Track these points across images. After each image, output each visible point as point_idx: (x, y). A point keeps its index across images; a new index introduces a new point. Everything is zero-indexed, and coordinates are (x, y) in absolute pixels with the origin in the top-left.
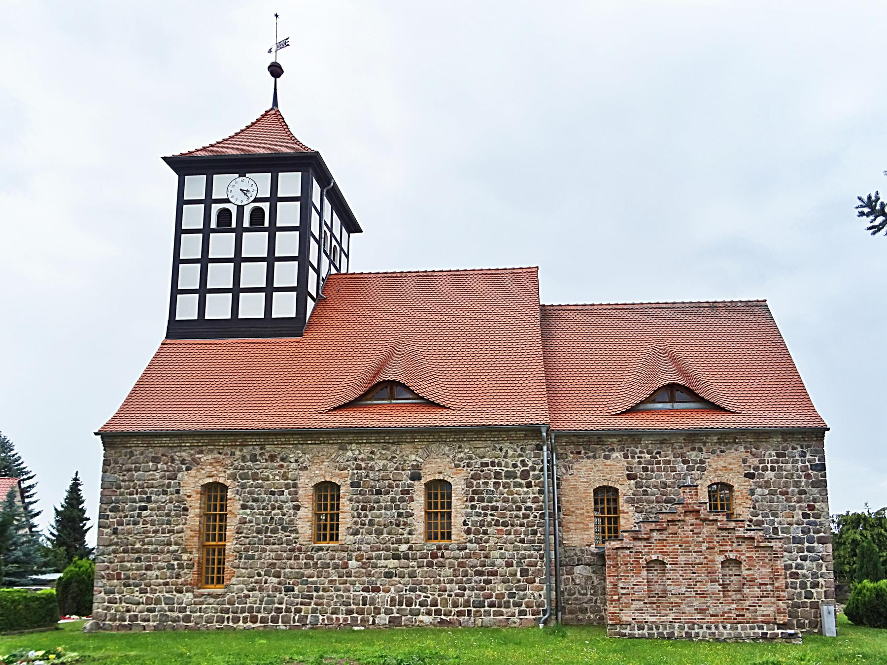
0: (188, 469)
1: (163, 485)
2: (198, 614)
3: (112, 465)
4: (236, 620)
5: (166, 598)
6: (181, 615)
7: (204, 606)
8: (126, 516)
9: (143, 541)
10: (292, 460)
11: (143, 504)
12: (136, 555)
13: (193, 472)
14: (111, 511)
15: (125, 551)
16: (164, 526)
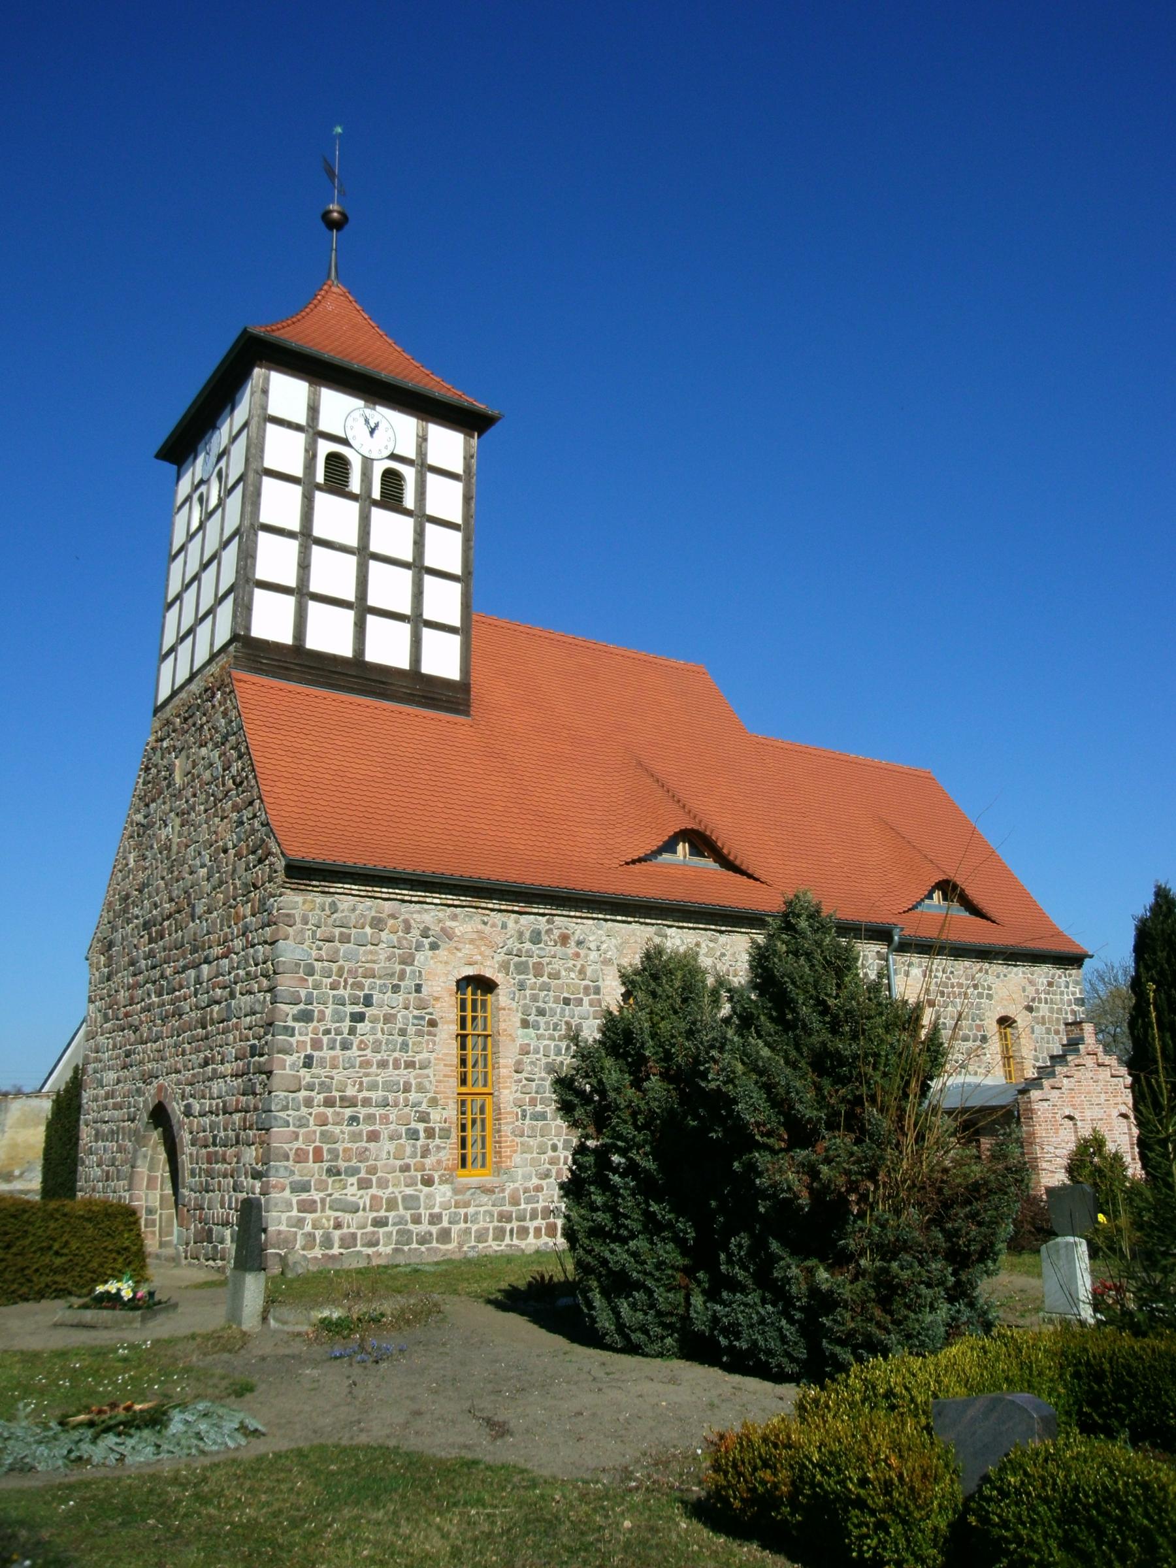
0: (434, 947)
1: (392, 975)
2: (463, 1225)
3: (299, 926)
4: (523, 1232)
5: (404, 1198)
6: (434, 1230)
7: (471, 1210)
8: (327, 1032)
9: (361, 1083)
10: (593, 946)
11: (357, 1009)
12: (348, 1112)
13: (442, 953)
14: (296, 1019)
15: (329, 1103)
16: (396, 1054)
